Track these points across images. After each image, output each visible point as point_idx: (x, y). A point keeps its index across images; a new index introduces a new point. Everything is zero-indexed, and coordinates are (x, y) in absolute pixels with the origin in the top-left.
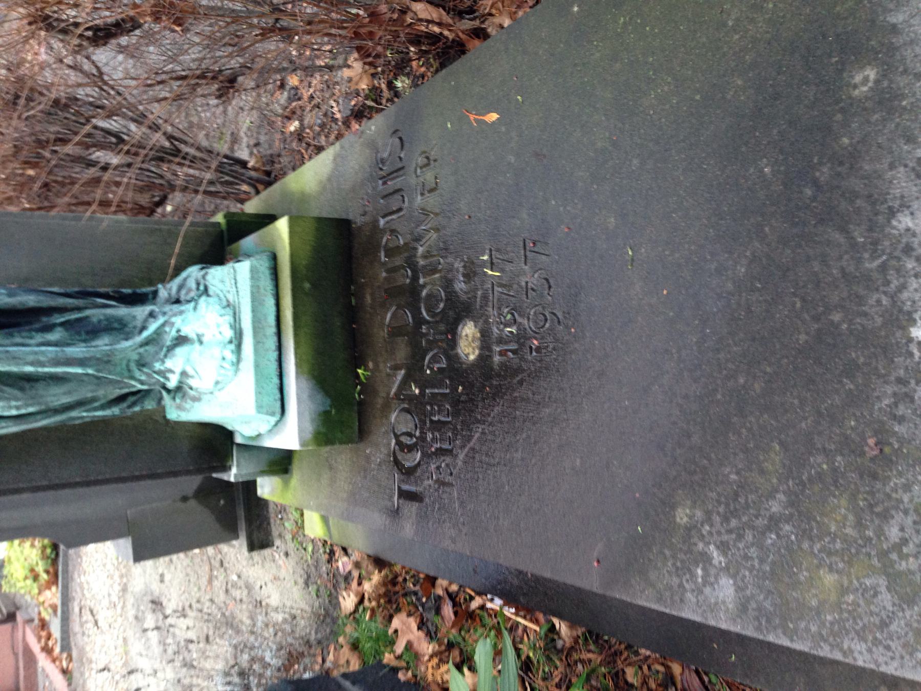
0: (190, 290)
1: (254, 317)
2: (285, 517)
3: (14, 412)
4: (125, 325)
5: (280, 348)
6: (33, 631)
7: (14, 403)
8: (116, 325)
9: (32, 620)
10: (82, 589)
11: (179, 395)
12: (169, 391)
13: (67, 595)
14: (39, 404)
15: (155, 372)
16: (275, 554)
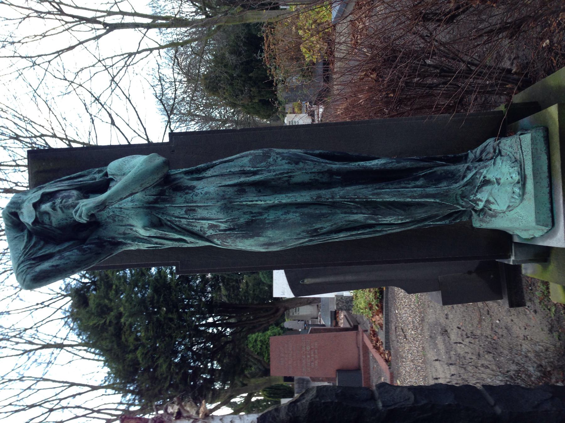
0: (488, 153)
1: (534, 167)
2: (534, 288)
3: (400, 222)
4: (454, 175)
5: (551, 185)
6: (368, 337)
7: (400, 217)
8: (450, 175)
9: (367, 331)
10: (396, 317)
11: (482, 213)
12: (476, 211)
13: (388, 320)
14: (412, 218)
15: (470, 201)
16: (527, 310)
